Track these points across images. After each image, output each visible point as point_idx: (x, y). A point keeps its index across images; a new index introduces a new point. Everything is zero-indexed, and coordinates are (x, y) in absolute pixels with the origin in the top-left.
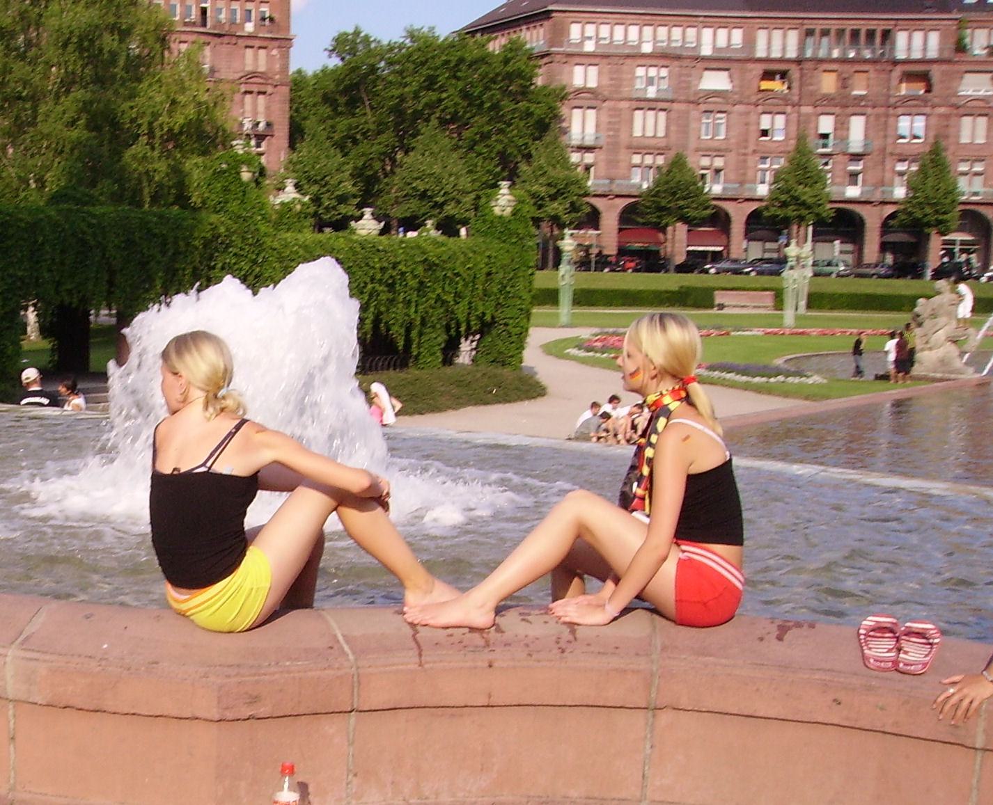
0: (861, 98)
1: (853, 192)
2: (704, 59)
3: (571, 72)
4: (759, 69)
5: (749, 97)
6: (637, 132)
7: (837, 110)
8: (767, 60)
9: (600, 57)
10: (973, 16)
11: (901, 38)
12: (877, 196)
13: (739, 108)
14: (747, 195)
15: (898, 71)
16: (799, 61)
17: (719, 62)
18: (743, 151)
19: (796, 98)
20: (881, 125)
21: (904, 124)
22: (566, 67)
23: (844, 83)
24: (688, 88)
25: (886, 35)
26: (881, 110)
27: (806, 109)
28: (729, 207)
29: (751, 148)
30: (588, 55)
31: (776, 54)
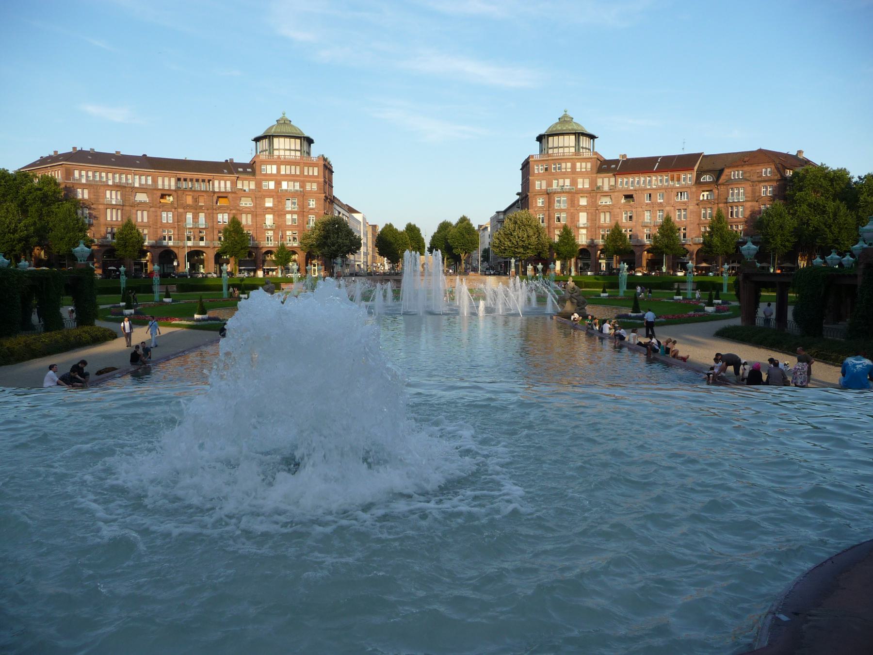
0: (202, 206)
1: (202, 244)
4: (159, 194)
6: (109, 219)
8: (163, 190)
9: (88, 186)
10: (241, 176)
11: (216, 183)
12: (211, 245)
13: (153, 209)
17: (143, 189)
20: (211, 217)
21: (220, 216)
23: (196, 200)
25: (209, 181)
27: (181, 210)
30: (83, 184)
31: (167, 187)
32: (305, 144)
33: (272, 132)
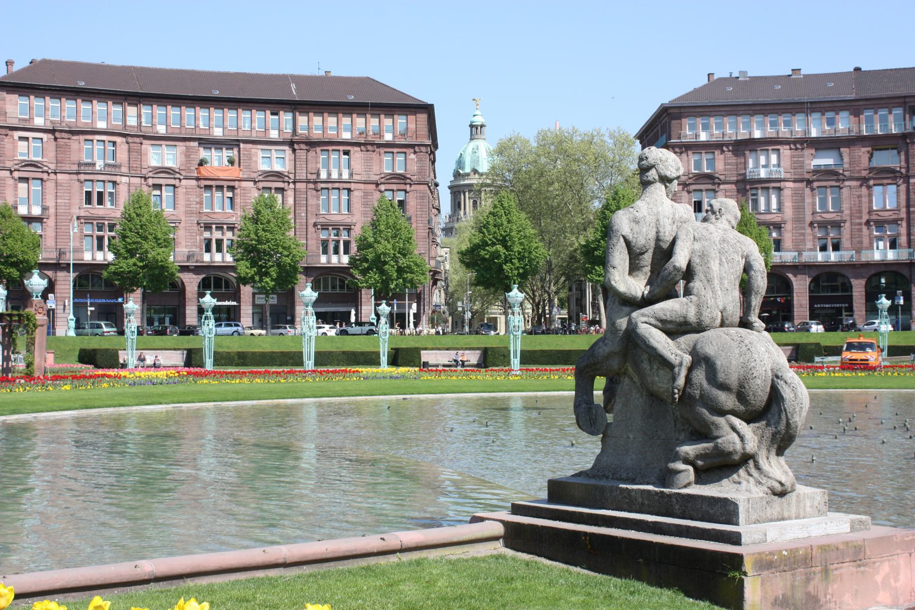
18: (858, 221)
24: (802, 167)
29: (865, 217)
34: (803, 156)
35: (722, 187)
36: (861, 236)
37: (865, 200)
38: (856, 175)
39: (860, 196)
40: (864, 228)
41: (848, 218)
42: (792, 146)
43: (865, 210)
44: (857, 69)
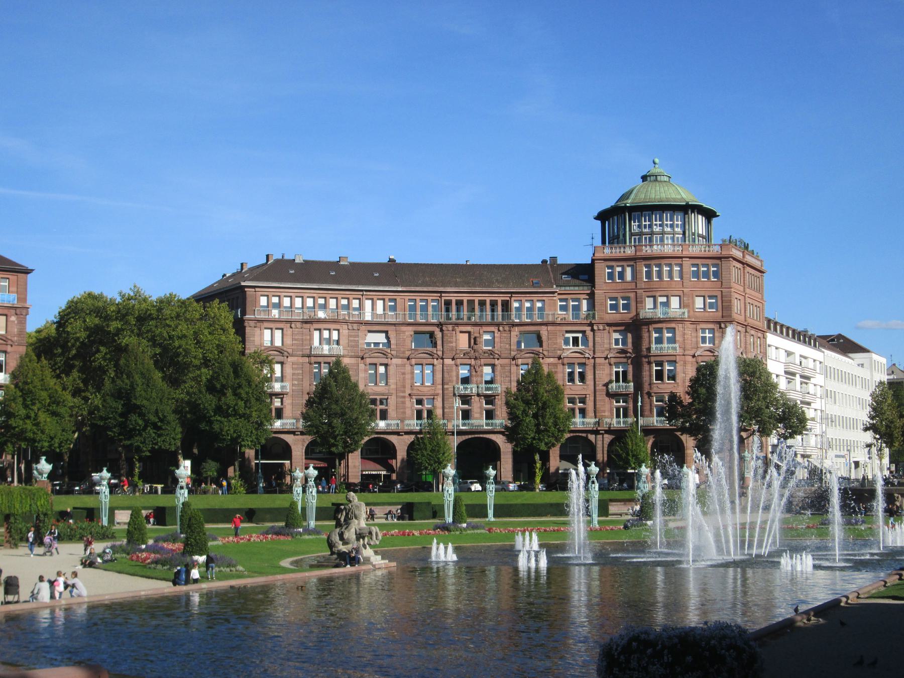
2: (367, 323)
3: (262, 335)
5: (404, 352)
7: (473, 362)
14: (406, 428)
15: (516, 331)
16: (440, 325)
18: (402, 394)
19: (440, 353)
22: (257, 331)
23: (474, 341)
24: (357, 346)
26: (507, 361)
28: (393, 439)
29: (408, 391)
32: (699, 223)
33: (629, 202)
34: (357, 336)
35: (290, 359)
36: (405, 408)
37: (408, 376)
38: (402, 355)
39: (404, 374)
40: (408, 399)
41: (394, 392)
42: (350, 327)
43: (408, 386)
44: (391, 260)
